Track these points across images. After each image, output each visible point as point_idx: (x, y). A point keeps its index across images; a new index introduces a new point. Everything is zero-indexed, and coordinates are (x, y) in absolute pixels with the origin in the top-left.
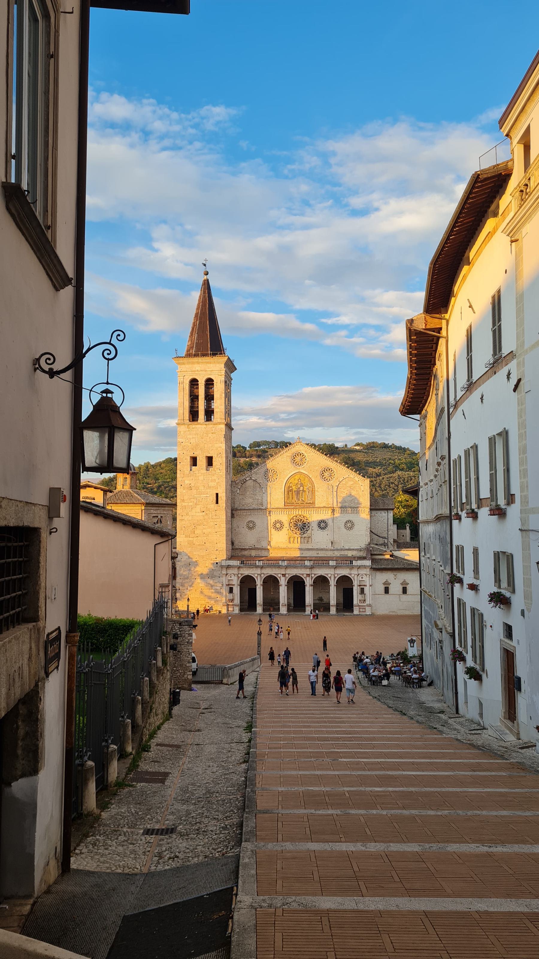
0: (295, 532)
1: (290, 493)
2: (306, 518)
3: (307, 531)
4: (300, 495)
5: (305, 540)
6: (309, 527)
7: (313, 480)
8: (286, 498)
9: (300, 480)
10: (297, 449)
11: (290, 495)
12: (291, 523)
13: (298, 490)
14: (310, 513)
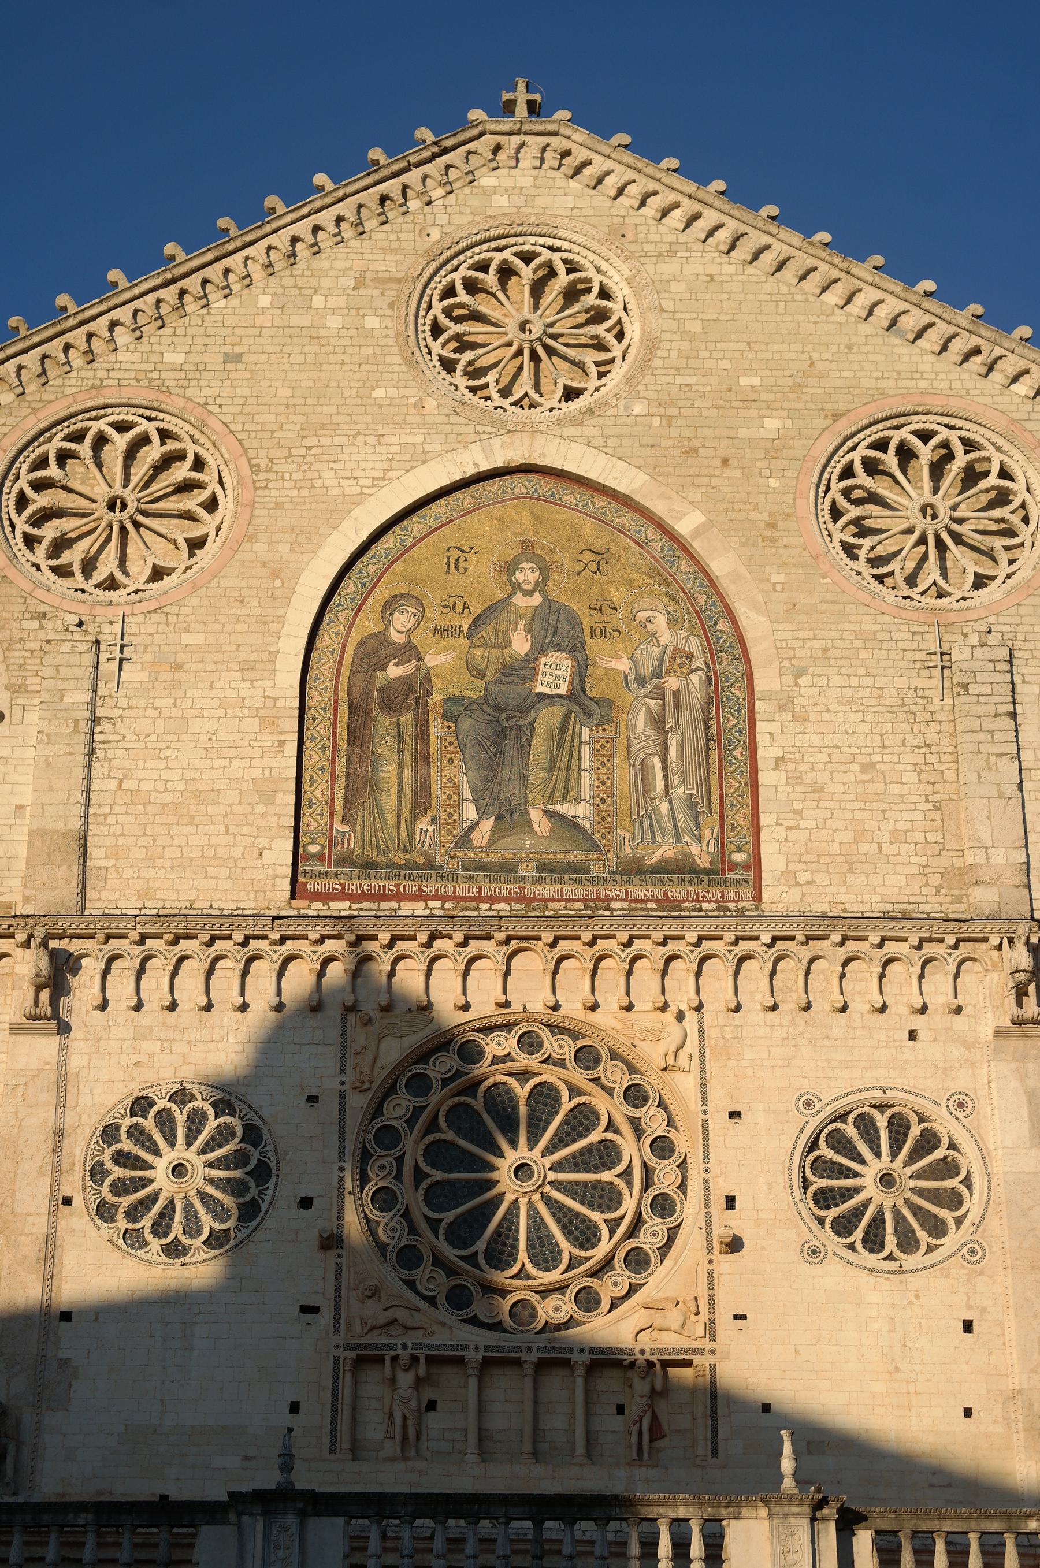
0: (438, 1283)
1: (384, 722)
2: (621, 1080)
3: (637, 1261)
4: (540, 744)
5: (609, 1423)
6: (663, 1206)
7: (719, 566)
8: (317, 791)
9: (527, 575)
10: (502, 202)
11: (384, 745)
12: (388, 1137)
13: (510, 694)
14: (682, 995)
